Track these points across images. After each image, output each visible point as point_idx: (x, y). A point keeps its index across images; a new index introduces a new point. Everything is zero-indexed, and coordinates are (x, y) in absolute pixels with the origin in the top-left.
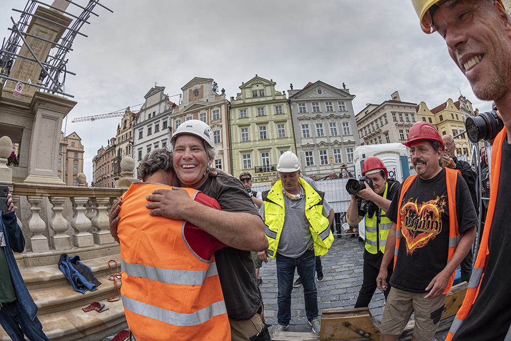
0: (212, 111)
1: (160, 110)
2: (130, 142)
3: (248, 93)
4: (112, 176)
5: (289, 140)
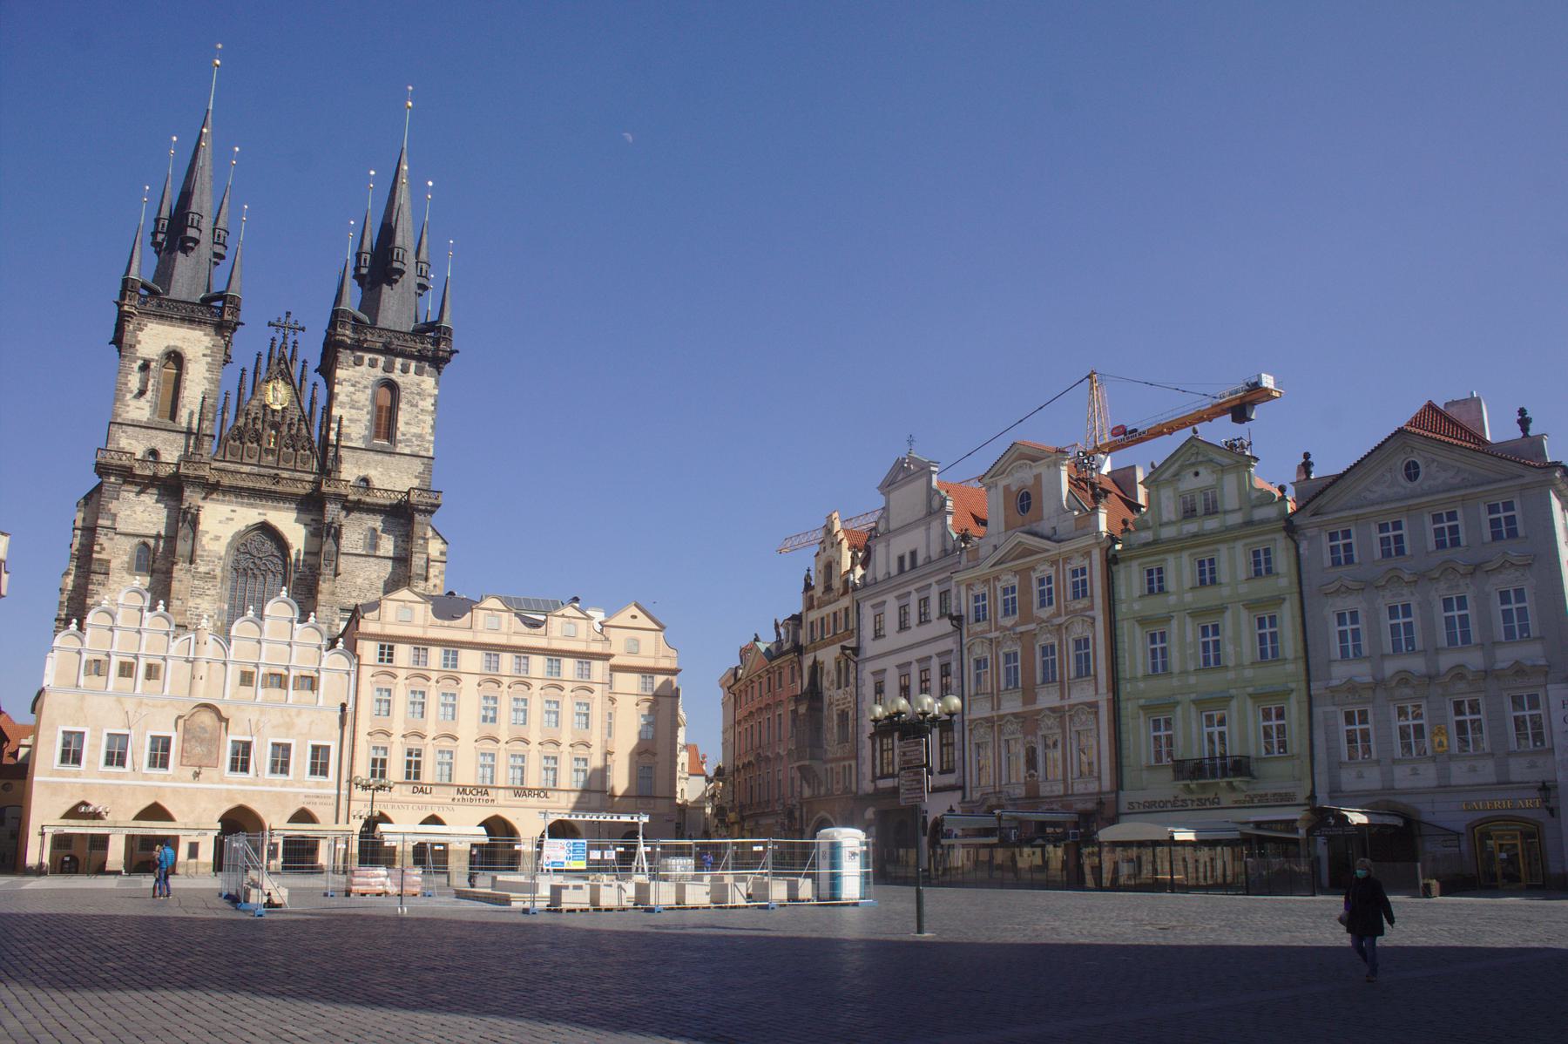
0: (1068, 567)
1: (928, 546)
4: (790, 753)
5: (1290, 667)
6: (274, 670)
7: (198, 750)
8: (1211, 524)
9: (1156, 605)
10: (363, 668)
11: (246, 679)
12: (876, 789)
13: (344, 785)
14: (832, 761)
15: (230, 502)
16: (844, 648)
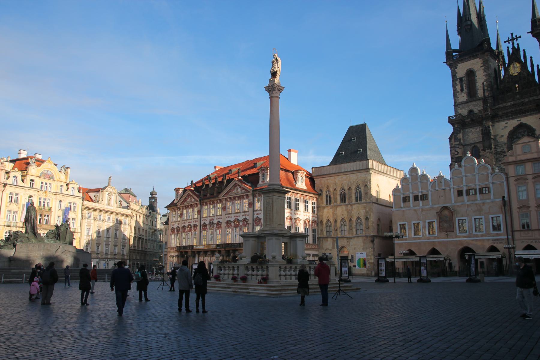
6: (470, 188)
7: (446, 225)
10: (510, 179)
11: (460, 193)
13: (510, 233)
15: (504, 120)
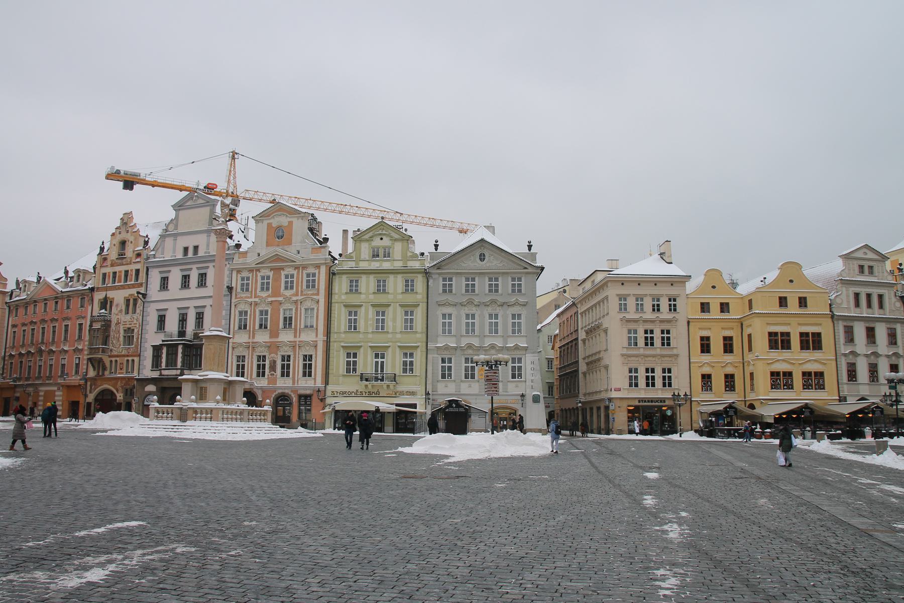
0: (305, 272)
1: (208, 245)
2: (138, 293)
3: (365, 250)
5: (418, 336)
8: (386, 265)
9: (354, 299)
12: (161, 375)
14: (117, 356)
16: (138, 293)
